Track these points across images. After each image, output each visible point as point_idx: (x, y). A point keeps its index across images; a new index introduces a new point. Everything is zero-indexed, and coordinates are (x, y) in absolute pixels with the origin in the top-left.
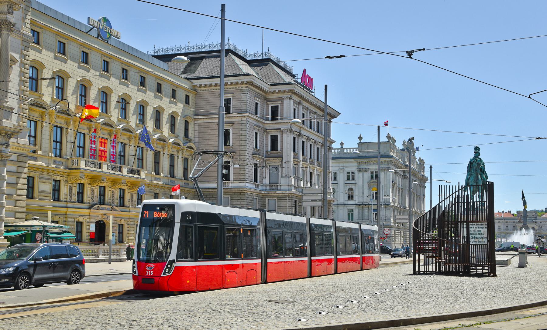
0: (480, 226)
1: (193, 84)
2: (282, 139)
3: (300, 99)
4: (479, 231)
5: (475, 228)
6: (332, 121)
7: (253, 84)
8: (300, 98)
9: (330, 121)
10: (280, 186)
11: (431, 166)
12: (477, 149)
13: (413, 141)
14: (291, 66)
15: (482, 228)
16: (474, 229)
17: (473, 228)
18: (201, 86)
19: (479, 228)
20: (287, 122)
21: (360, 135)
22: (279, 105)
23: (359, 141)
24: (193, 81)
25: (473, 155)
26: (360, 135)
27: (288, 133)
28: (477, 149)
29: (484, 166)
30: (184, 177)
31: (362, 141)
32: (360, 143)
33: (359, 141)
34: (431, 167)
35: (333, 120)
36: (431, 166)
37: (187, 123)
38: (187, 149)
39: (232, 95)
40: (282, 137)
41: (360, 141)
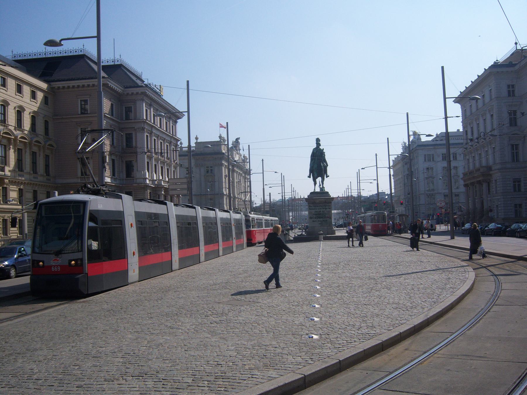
0: (324, 207)
1: (51, 86)
2: (136, 137)
3: (151, 101)
4: (323, 211)
5: (320, 209)
6: (178, 122)
7: (108, 86)
8: (151, 100)
9: (176, 122)
10: (136, 179)
11: (263, 159)
12: (318, 140)
13: (239, 140)
14: (140, 72)
15: (326, 209)
16: (319, 210)
17: (319, 209)
18: (59, 88)
19: (323, 209)
20: (140, 122)
22: (133, 106)
24: (52, 83)
25: (315, 146)
27: (141, 131)
28: (318, 140)
29: (325, 155)
30: (46, 173)
31: (198, 141)
32: (197, 142)
33: (196, 141)
34: (263, 160)
36: (263, 159)
37: (46, 123)
38: (48, 147)
39: (88, 96)
40: (136, 135)
41: (197, 140)
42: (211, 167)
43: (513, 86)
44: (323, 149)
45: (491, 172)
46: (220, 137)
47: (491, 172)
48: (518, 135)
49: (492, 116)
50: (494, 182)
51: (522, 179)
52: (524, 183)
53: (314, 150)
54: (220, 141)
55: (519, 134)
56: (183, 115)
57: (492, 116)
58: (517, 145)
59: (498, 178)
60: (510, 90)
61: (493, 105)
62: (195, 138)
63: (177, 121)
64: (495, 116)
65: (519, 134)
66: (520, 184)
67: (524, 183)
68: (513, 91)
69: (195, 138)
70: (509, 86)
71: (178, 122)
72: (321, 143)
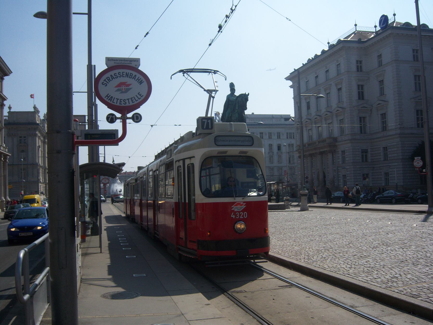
6: (4, 79)
12: (232, 86)
21: (10, 105)
23: (9, 110)
25: (229, 93)
26: (10, 105)
28: (232, 86)
31: (12, 110)
33: (9, 110)
35: (6, 78)
42: (25, 137)
43: (361, 62)
44: (248, 94)
45: (337, 144)
46: (35, 107)
47: (337, 144)
48: (366, 108)
49: (339, 89)
50: (340, 152)
51: (369, 150)
52: (371, 154)
53: (228, 97)
54: (35, 111)
55: (367, 107)
56: (11, 72)
57: (339, 89)
58: (364, 118)
59: (346, 149)
60: (358, 66)
61: (343, 79)
62: (9, 107)
63: (4, 78)
64: (344, 90)
65: (367, 107)
66: (367, 155)
67: (371, 154)
68: (361, 67)
69: (9, 107)
70: (357, 61)
71: (4, 79)
72: (236, 88)
